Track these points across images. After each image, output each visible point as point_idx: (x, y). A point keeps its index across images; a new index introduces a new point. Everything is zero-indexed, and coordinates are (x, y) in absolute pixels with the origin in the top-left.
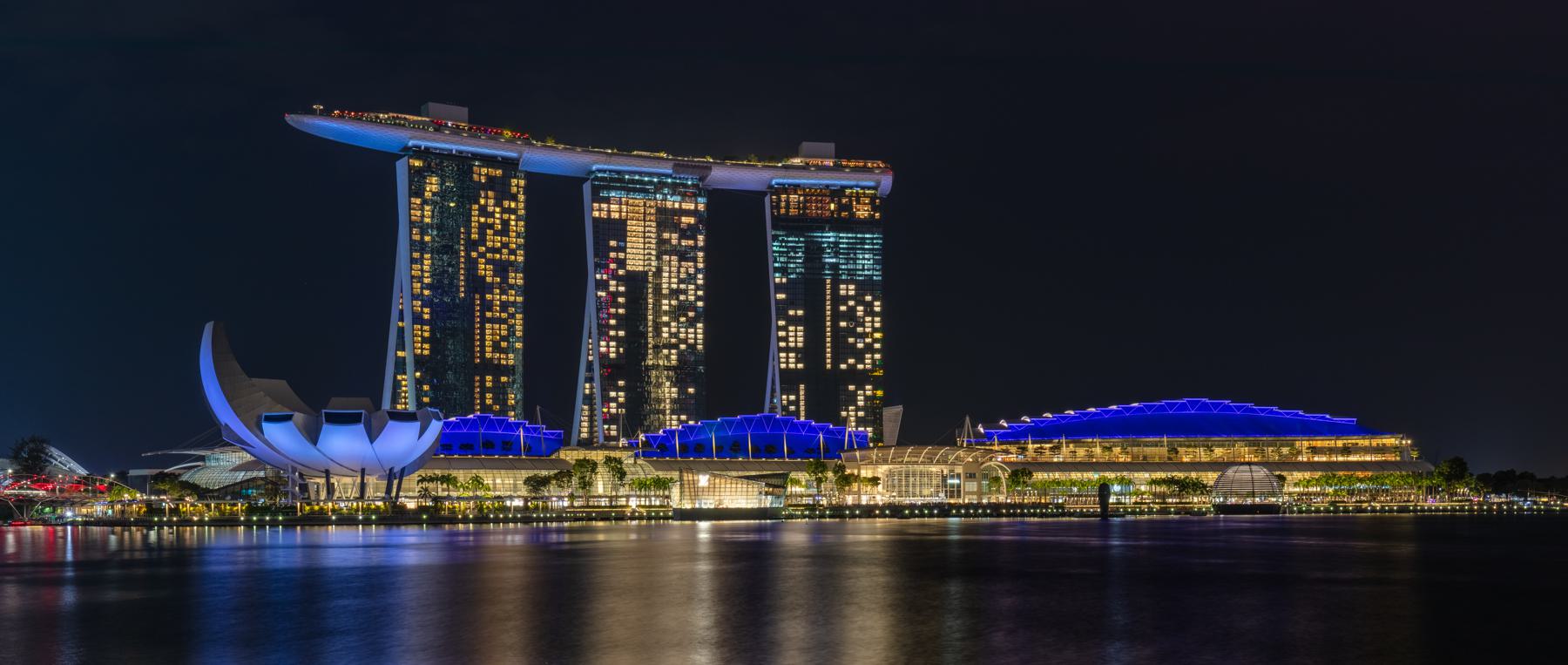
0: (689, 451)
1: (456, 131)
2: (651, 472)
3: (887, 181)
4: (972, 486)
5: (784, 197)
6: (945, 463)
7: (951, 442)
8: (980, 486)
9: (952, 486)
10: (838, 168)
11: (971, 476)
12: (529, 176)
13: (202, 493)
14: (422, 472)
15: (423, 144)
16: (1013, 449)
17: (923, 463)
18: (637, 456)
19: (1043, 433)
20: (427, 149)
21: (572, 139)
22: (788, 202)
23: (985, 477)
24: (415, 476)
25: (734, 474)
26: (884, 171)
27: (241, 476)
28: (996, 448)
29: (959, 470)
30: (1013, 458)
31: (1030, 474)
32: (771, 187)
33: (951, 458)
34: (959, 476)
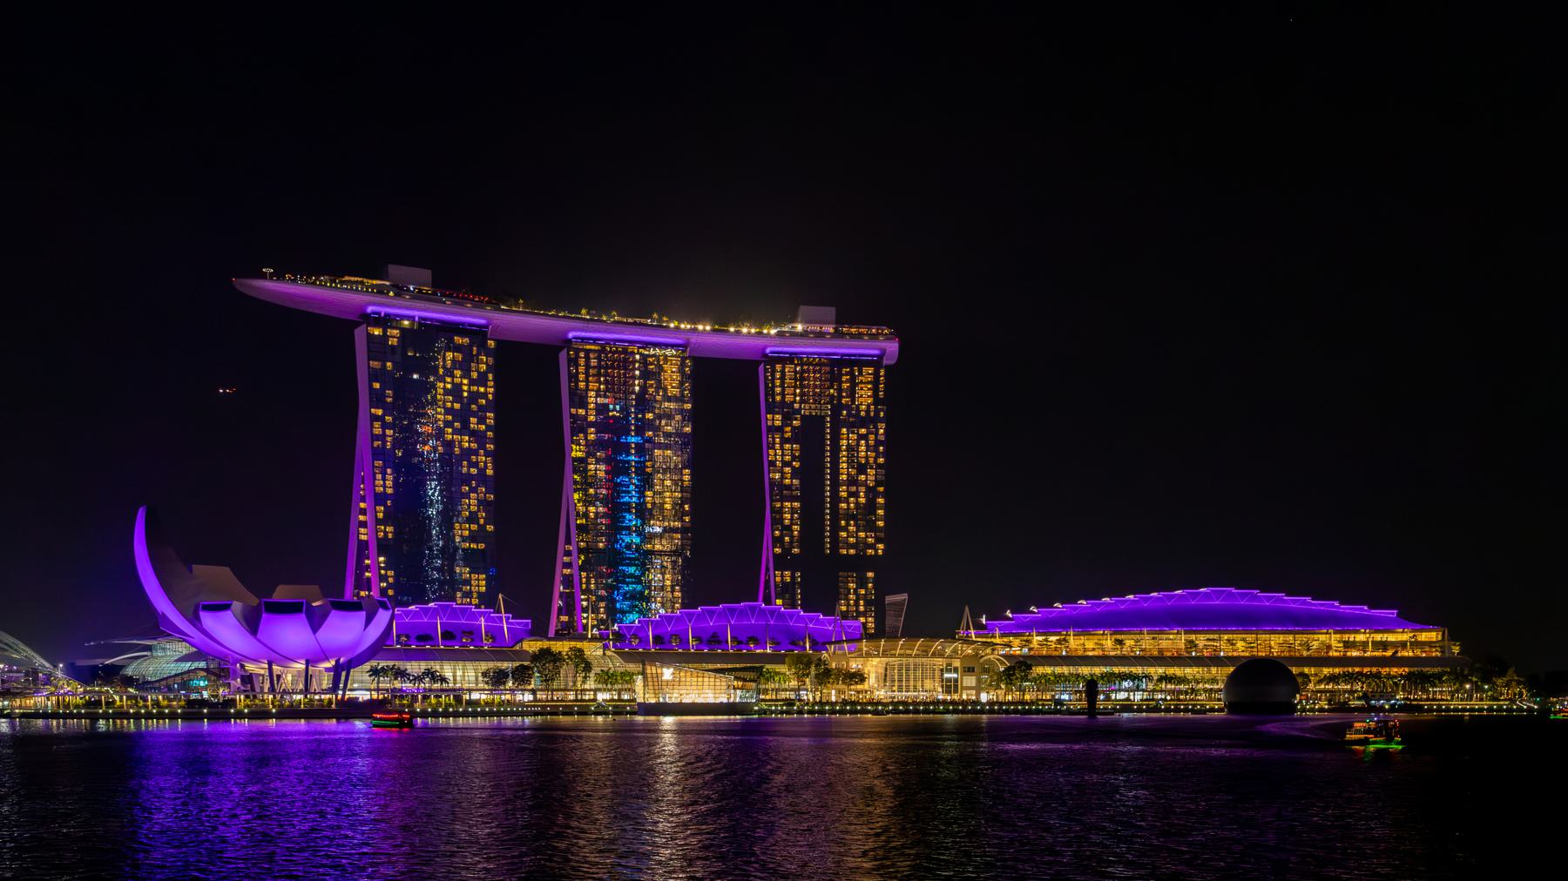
0: (663, 645)
1: (419, 296)
2: (617, 664)
3: (893, 347)
4: (970, 681)
5: (778, 367)
6: (941, 655)
7: (951, 636)
8: (979, 681)
9: (949, 680)
10: (838, 335)
11: (969, 670)
12: (498, 342)
13: (144, 685)
14: (374, 663)
15: (383, 310)
16: (1016, 642)
17: (917, 656)
18: (606, 647)
19: (1046, 626)
20: (387, 315)
21: (542, 300)
22: (783, 372)
23: (986, 671)
24: (367, 666)
25: (710, 666)
26: (888, 338)
27: (187, 666)
28: (998, 640)
29: (957, 663)
30: (1016, 650)
31: (1030, 667)
32: (766, 355)
33: (948, 651)
34: (956, 670)
